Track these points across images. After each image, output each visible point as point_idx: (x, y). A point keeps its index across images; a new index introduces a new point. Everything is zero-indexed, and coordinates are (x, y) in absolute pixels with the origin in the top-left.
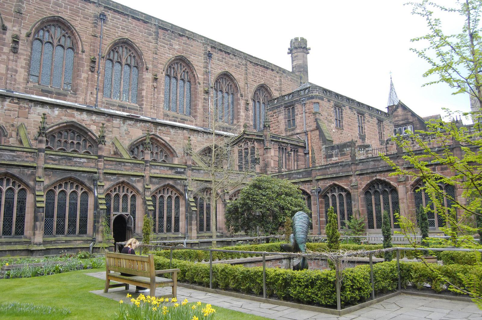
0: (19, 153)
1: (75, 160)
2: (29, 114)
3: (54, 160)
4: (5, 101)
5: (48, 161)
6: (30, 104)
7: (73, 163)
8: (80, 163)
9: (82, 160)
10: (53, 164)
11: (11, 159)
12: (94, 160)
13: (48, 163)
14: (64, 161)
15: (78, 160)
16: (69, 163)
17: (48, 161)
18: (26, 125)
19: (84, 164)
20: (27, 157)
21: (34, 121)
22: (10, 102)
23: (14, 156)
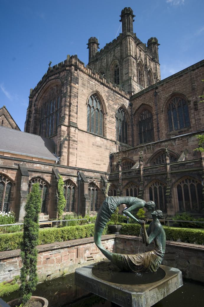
0: (159, 168)
1: (187, 165)
2: (188, 143)
3: (175, 168)
4: (176, 141)
5: (173, 169)
6: (187, 137)
7: (186, 167)
8: (190, 166)
9: (191, 164)
10: (175, 170)
11: (156, 172)
12: (199, 162)
13: (173, 170)
14: (181, 167)
15: (189, 164)
16: (184, 167)
17: (173, 169)
18: (188, 149)
19: (193, 166)
20: (163, 169)
21: (192, 145)
22: (178, 140)
23: (157, 170)
